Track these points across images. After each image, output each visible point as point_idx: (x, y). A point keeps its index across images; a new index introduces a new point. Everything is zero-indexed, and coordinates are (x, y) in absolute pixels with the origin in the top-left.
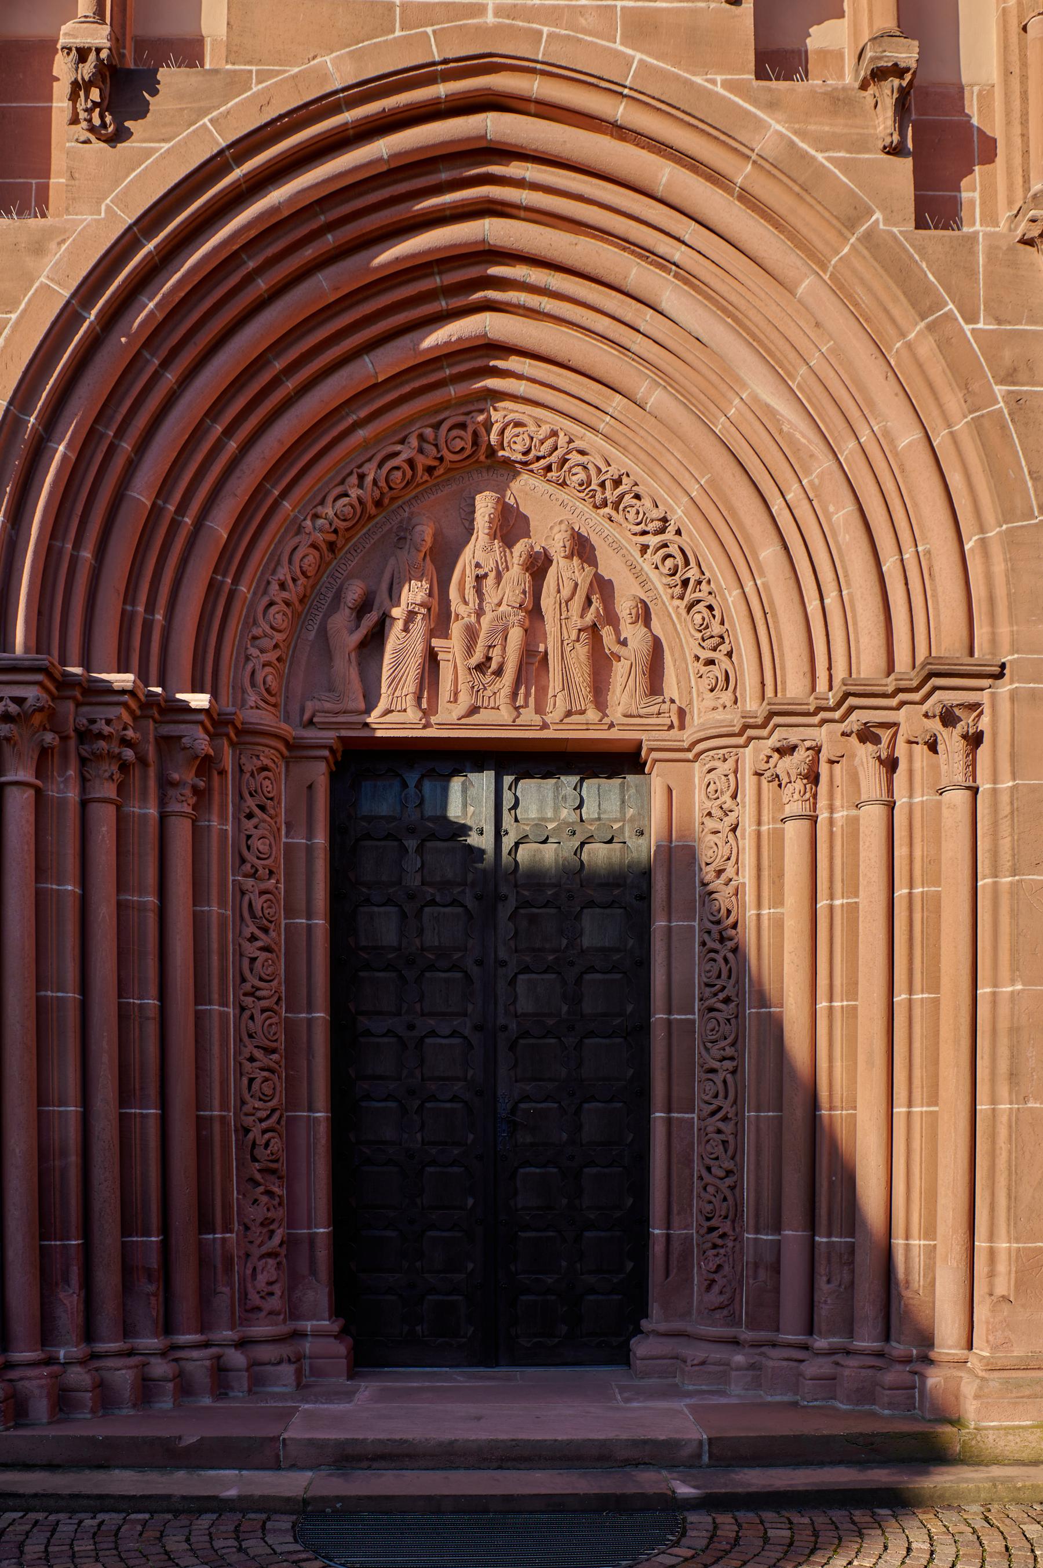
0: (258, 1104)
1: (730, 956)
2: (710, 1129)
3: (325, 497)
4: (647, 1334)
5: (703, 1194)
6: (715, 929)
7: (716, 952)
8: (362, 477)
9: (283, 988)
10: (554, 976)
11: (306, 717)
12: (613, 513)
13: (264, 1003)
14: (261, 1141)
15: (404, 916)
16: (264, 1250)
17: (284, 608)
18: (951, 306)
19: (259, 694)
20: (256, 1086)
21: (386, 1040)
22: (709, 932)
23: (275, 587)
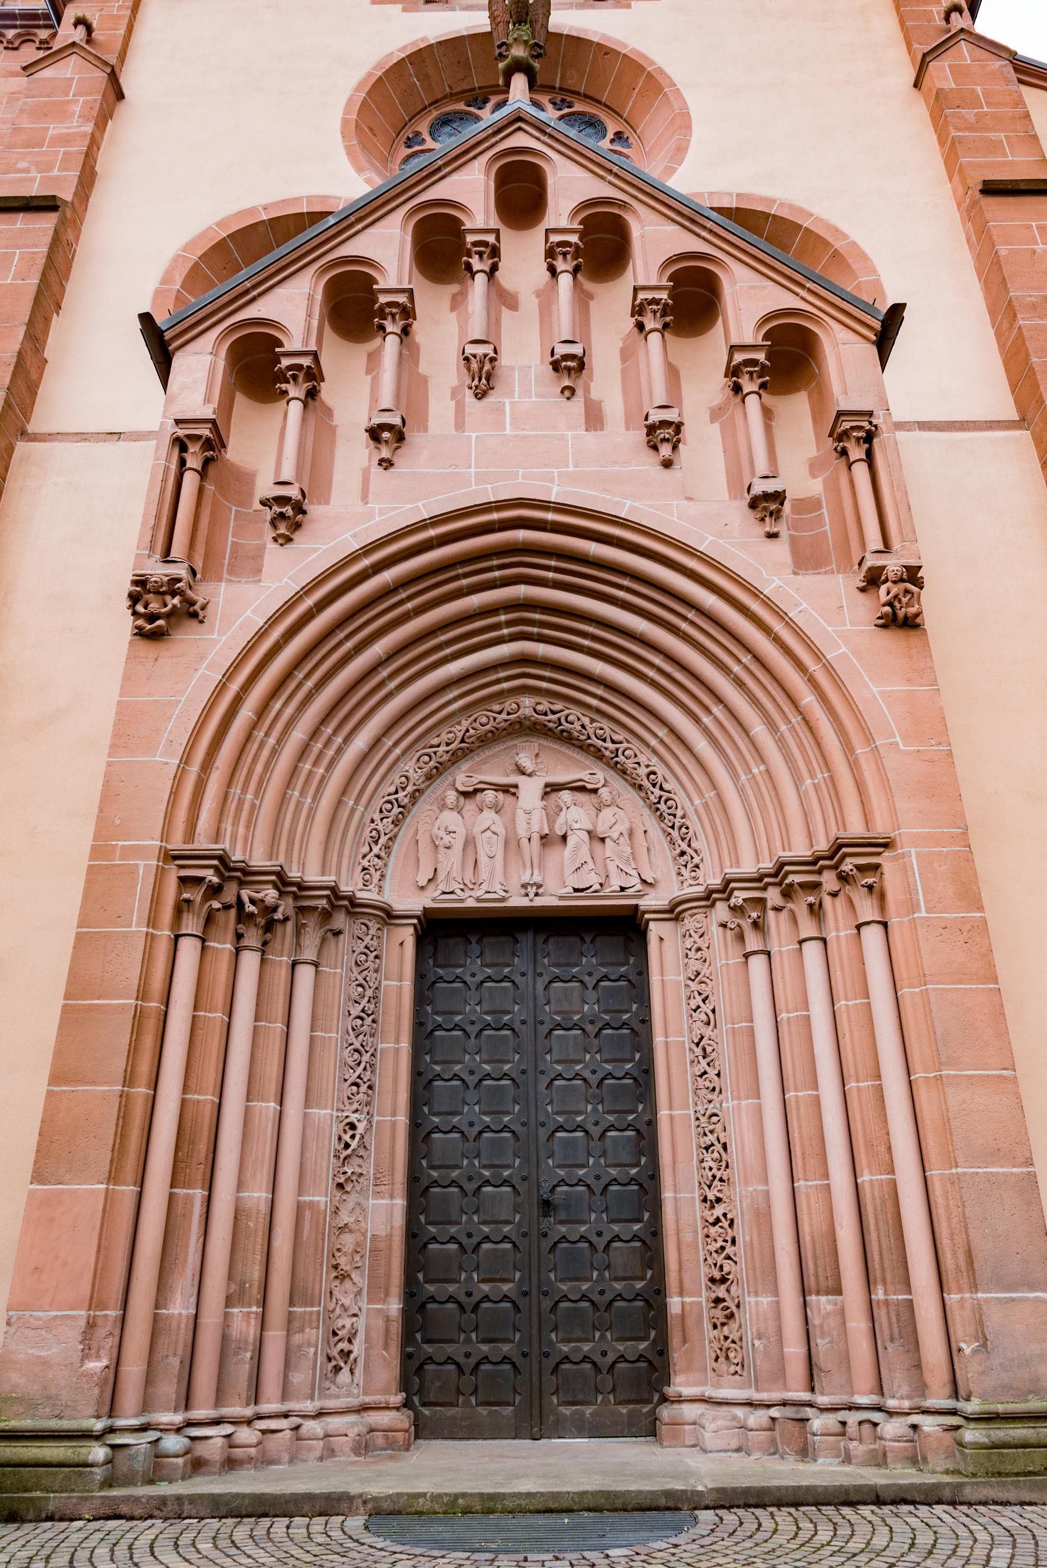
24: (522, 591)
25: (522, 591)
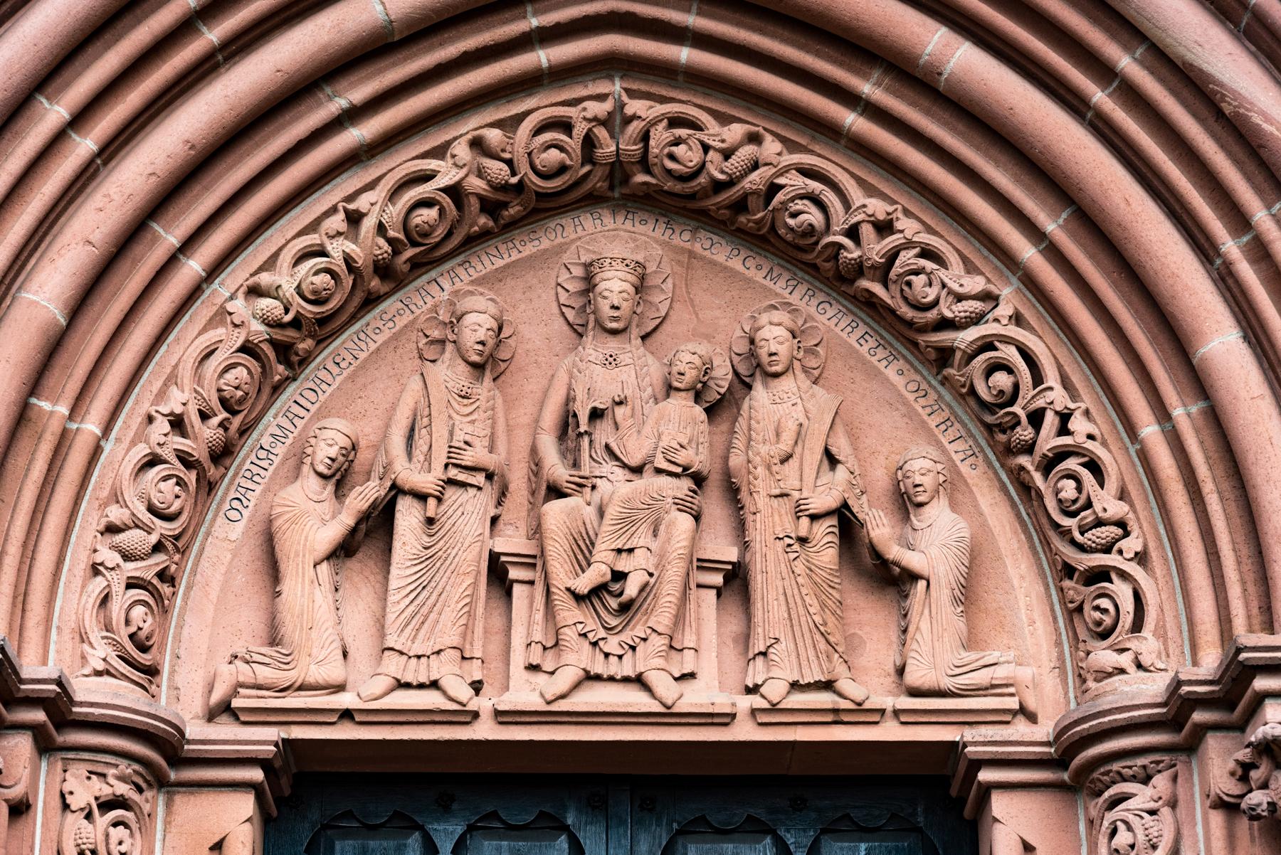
3: (275, 256)
8: (354, 219)
12: (877, 289)
17: (180, 469)
19: (116, 644)
23: (162, 425)
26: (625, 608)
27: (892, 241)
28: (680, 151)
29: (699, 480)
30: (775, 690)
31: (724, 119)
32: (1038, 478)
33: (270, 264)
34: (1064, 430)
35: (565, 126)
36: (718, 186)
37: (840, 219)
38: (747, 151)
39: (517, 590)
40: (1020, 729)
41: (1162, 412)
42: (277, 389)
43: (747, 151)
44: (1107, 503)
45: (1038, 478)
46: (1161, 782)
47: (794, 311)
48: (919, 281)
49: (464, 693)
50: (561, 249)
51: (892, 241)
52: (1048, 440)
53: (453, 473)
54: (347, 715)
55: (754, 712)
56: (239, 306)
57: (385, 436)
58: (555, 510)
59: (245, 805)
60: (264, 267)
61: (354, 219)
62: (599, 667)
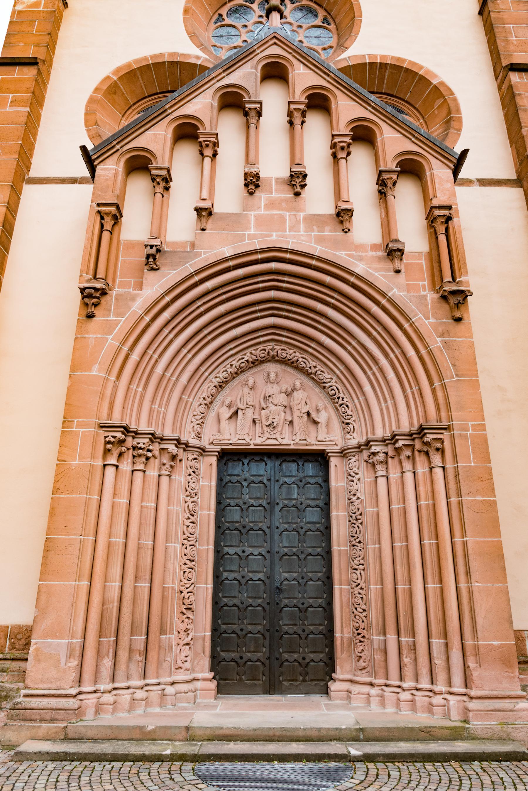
0: (187, 582)
1: (360, 525)
2: (356, 592)
4: (334, 680)
5: (354, 619)
6: (354, 515)
7: (355, 524)
8: (232, 365)
9: (198, 537)
10: (295, 533)
11: (210, 441)
12: (314, 376)
13: (191, 543)
14: (187, 596)
15: (242, 510)
16: (185, 642)
18: (421, 315)
20: (186, 574)
21: (234, 556)
22: (352, 517)
23: (202, 399)
24: (273, 294)
25: (273, 294)
26: (274, 427)
27: (316, 369)
28: (283, 354)
29: (285, 407)
30: (297, 441)
31: (290, 349)
32: (339, 408)
33: (218, 373)
34: (343, 400)
35: (265, 350)
36: (289, 360)
37: (308, 366)
38: (294, 354)
39: (257, 424)
40: (335, 447)
41: (358, 398)
42: (219, 392)
43: (294, 354)
44: (349, 412)
45: (339, 408)
46: (356, 457)
47: (301, 379)
48: (320, 376)
49: (249, 441)
50: (264, 369)
51: (316, 369)
52: (340, 402)
53: (247, 406)
54: (231, 444)
55: (294, 444)
56: (214, 380)
57: (236, 400)
58: (263, 411)
59: (215, 458)
60: (218, 373)
61: (232, 365)
62: (270, 437)
